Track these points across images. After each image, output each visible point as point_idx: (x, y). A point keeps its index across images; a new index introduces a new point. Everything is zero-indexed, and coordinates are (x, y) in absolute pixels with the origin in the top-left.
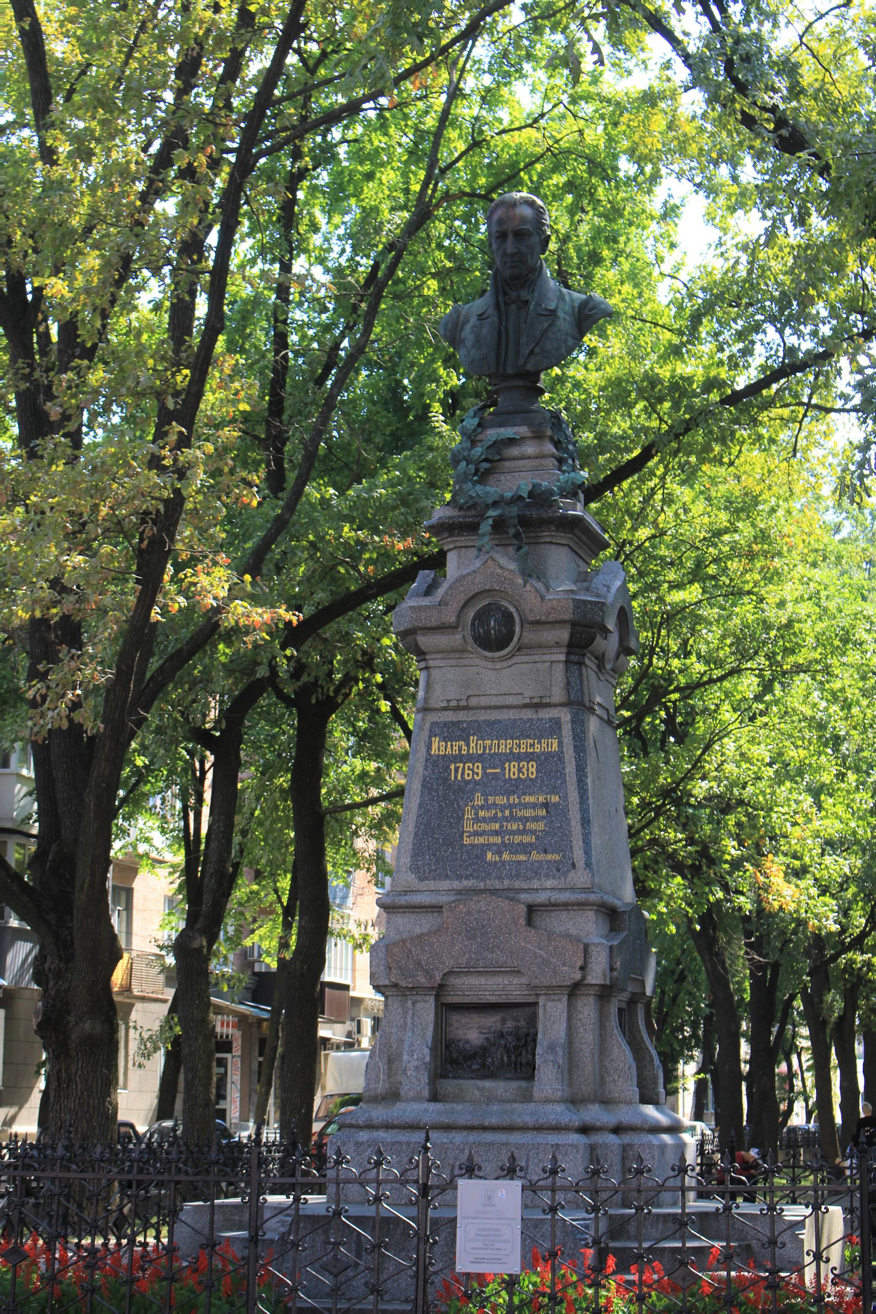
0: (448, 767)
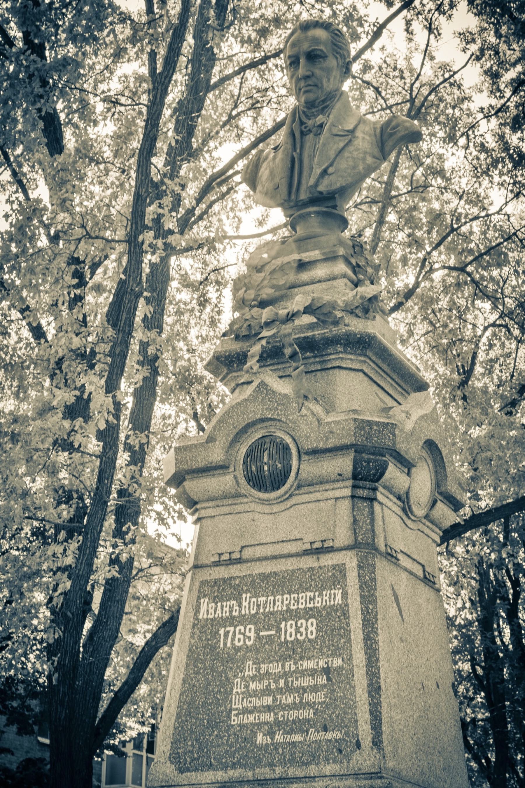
0: (217, 632)
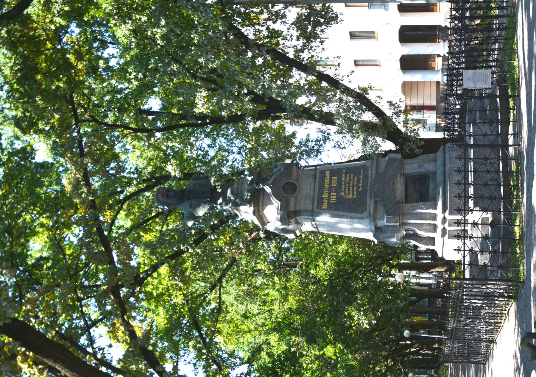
0: (332, 203)
